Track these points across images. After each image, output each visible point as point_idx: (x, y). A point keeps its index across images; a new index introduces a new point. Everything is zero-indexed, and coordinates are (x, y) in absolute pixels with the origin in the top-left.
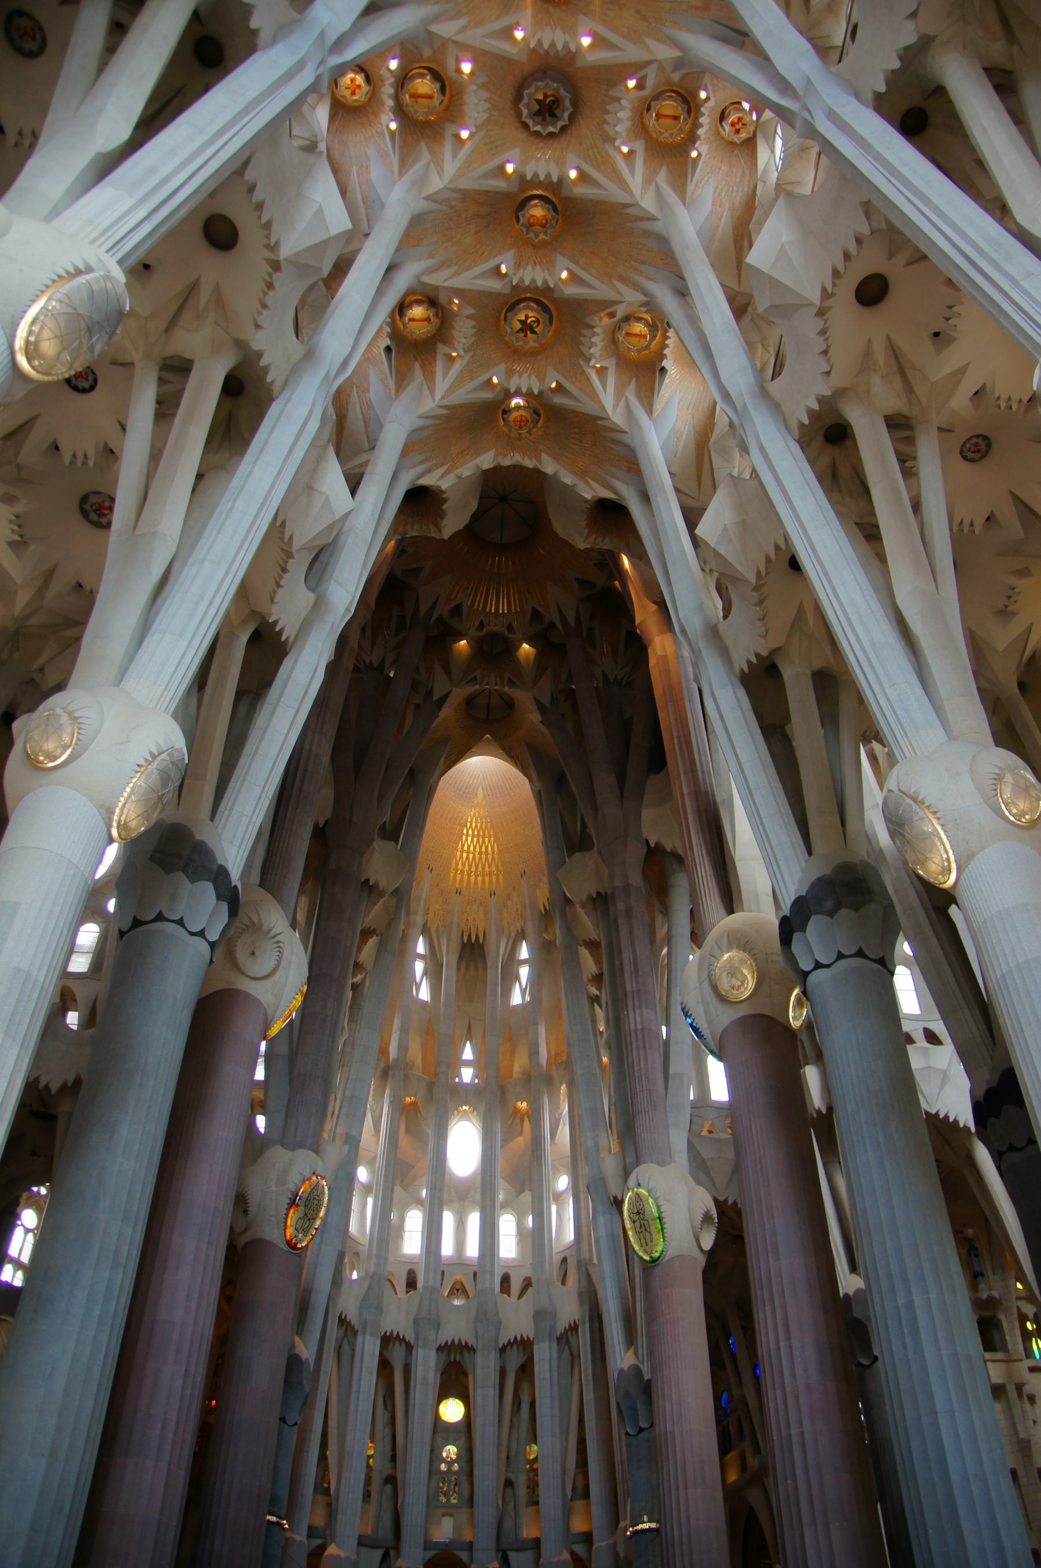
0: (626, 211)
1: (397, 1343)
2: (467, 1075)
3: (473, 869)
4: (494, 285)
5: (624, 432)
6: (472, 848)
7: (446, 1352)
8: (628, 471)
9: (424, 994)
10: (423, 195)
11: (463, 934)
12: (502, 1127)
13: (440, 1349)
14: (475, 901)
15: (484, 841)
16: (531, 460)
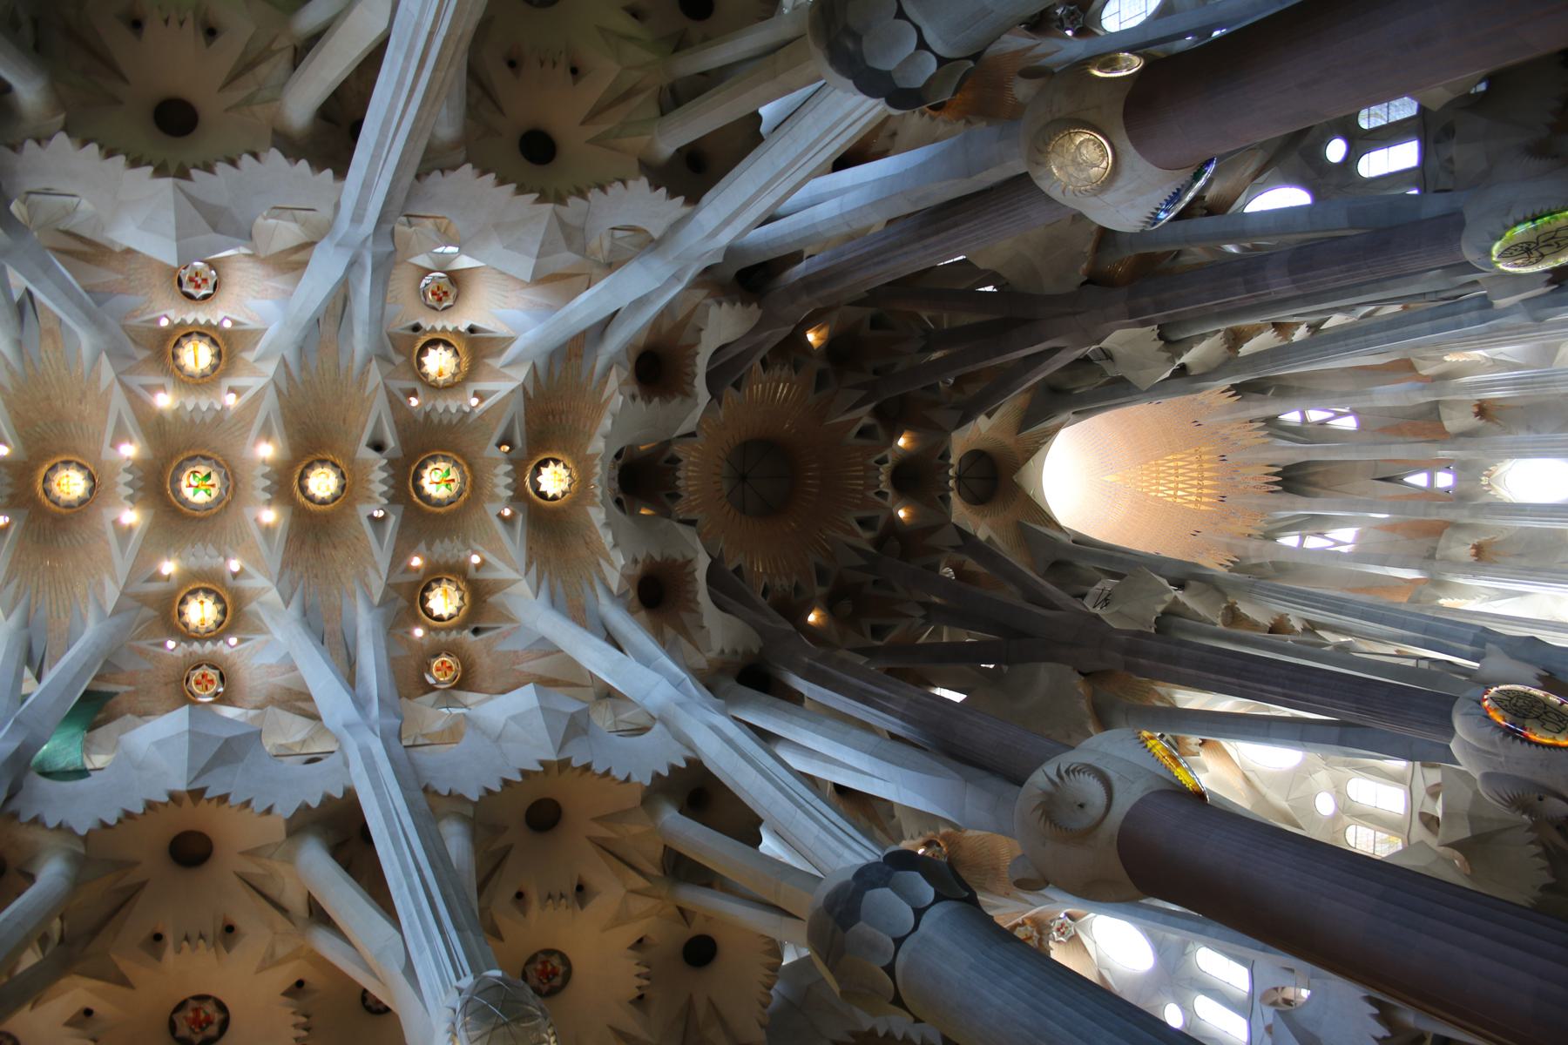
0: (285, 390)
2: (1444, 480)
3: (1195, 482)
4: (392, 521)
5: (534, 365)
6: (1172, 485)
8: (581, 356)
10: (284, 608)
11: (1272, 492)
15: (1163, 472)
16: (596, 465)
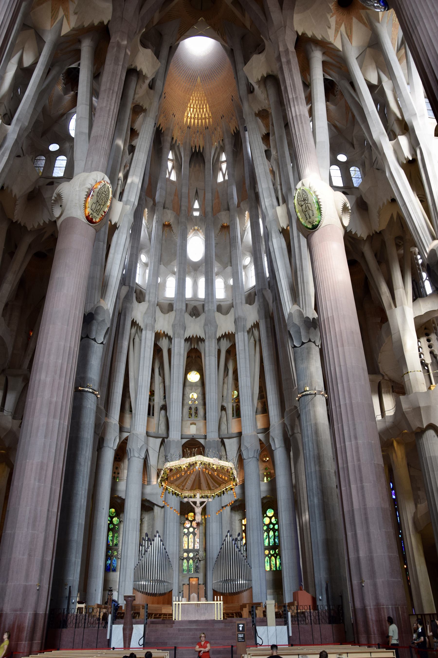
1: (164, 338)
3: (196, 116)
6: (195, 106)
7: (189, 343)
9: (173, 177)
11: (192, 148)
12: (215, 237)
13: (186, 340)
14: (198, 132)
